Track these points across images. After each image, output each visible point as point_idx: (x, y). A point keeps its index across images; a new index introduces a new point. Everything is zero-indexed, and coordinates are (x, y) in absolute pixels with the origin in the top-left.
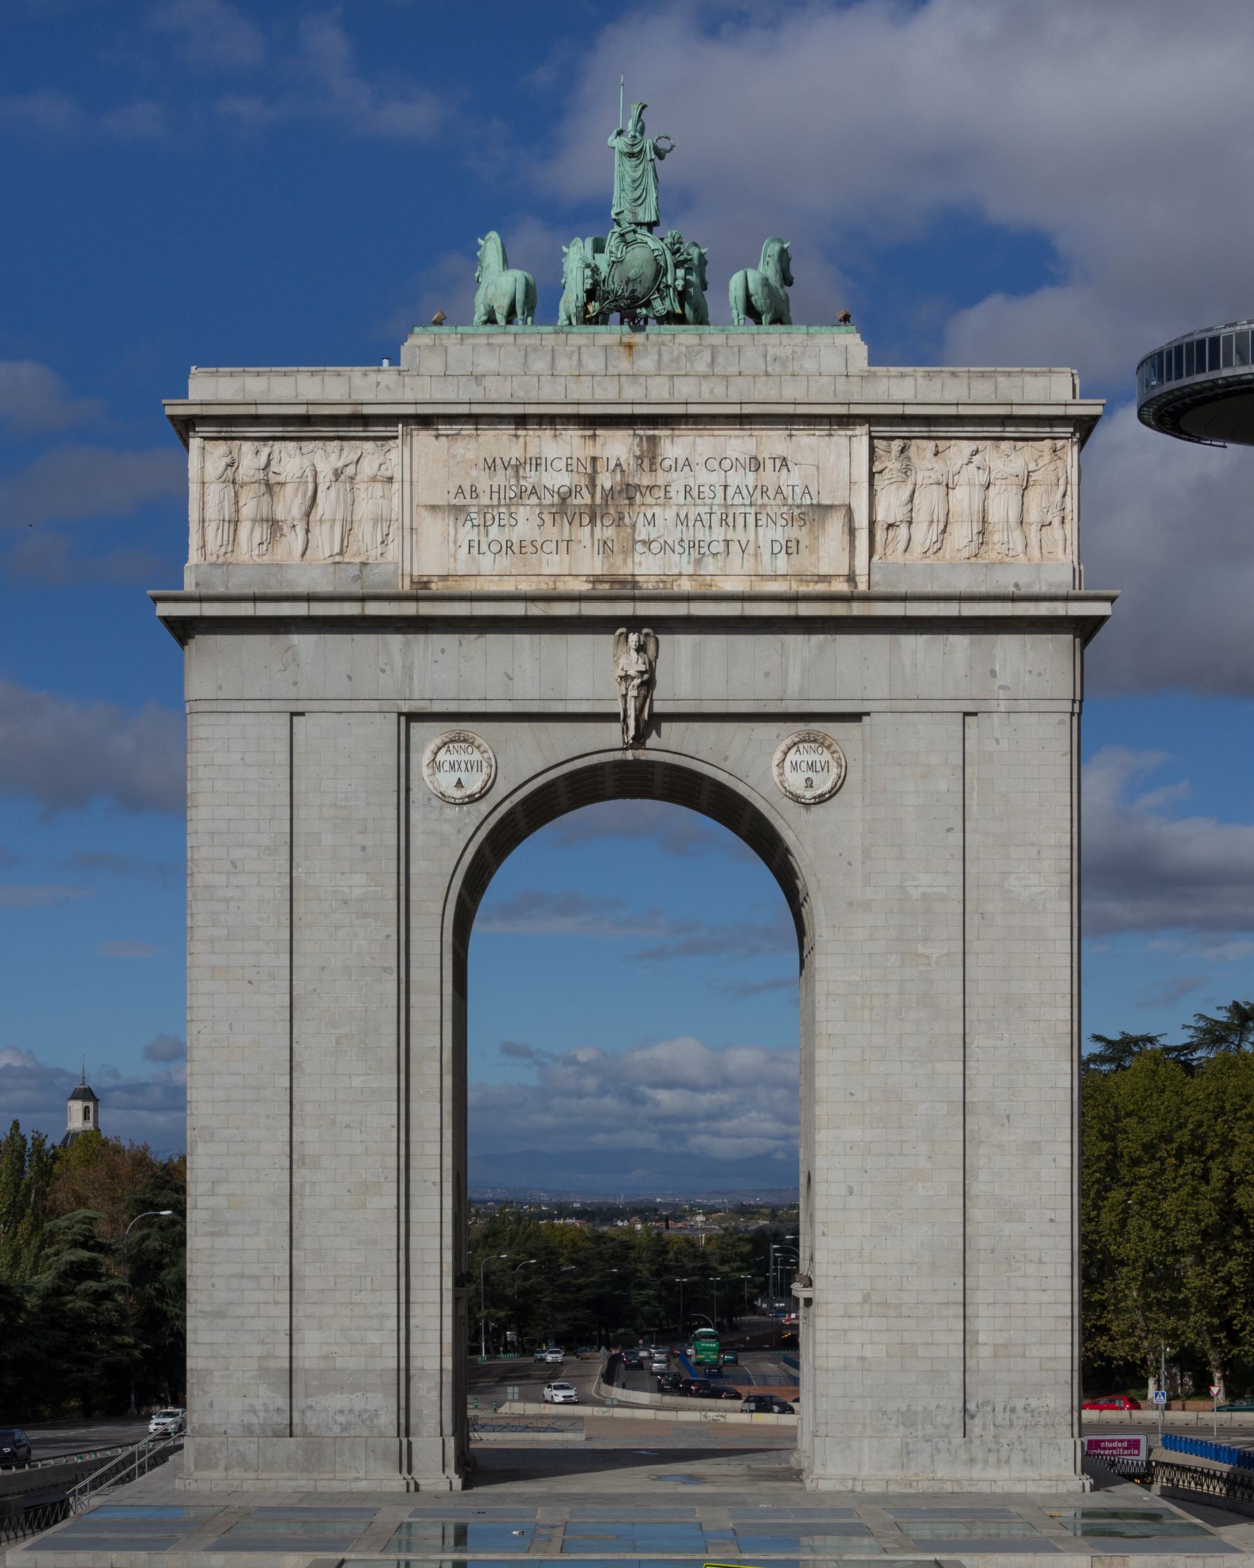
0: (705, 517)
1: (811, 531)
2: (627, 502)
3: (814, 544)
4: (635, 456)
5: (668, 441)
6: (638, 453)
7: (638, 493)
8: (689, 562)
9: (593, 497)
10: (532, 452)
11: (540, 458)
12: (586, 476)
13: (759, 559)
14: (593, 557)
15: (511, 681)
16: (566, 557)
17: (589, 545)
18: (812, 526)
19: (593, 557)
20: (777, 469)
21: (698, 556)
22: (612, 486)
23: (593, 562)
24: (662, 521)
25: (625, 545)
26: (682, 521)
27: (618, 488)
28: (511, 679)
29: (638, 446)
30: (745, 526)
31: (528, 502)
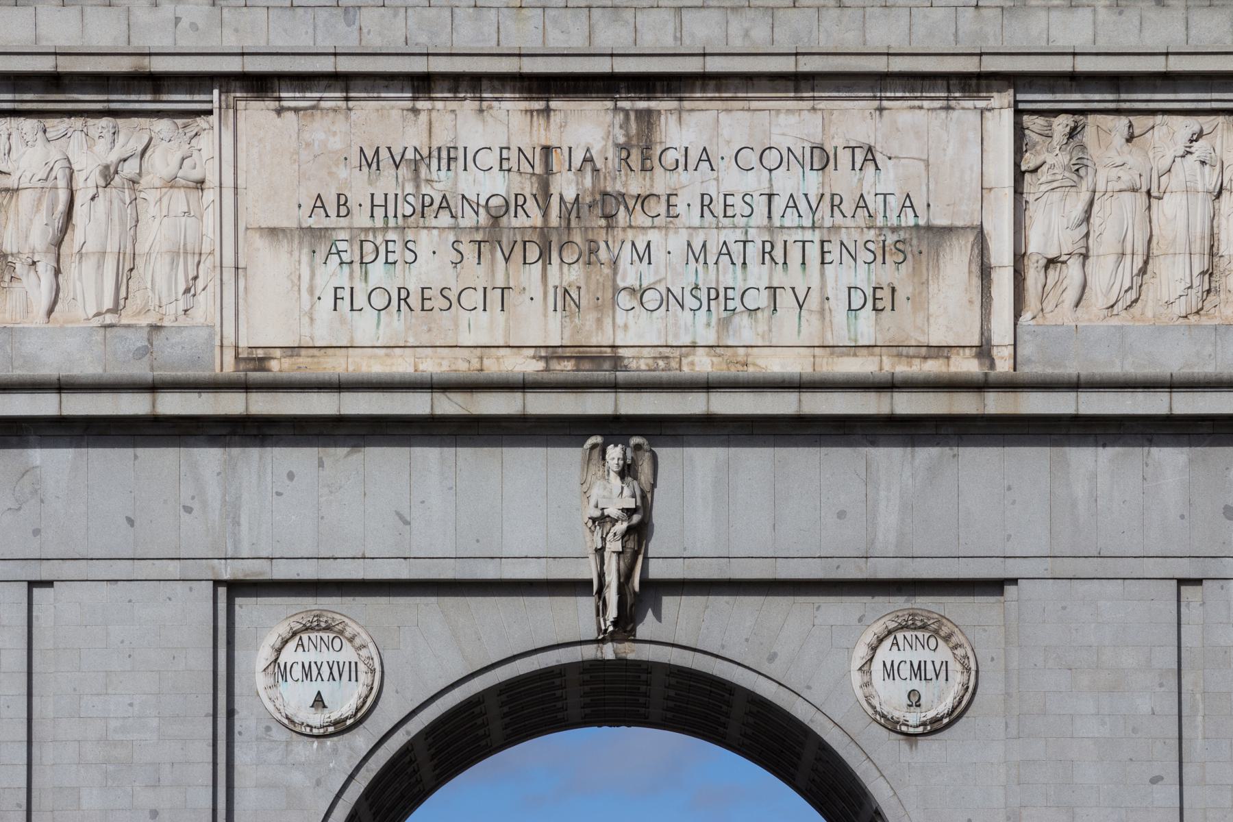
0: (736, 249)
1: (915, 271)
2: (603, 222)
3: (920, 293)
4: (617, 145)
5: (673, 119)
6: (621, 140)
7: (622, 208)
8: (708, 325)
9: (545, 215)
10: (442, 138)
11: (456, 148)
12: (534, 179)
13: (827, 319)
14: (545, 315)
15: (408, 527)
16: (501, 317)
17: (538, 296)
18: (917, 262)
19: (545, 315)
20: (858, 166)
21: (724, 315)
22: (578, 195)
23: (546, 324)
24: (663, 254)
25: (599, 295)
26: (698, 254)
27: (588, 200)
28: (407, 523)
29: (621, 127)
30: (804, 263)
31: (434, 223)
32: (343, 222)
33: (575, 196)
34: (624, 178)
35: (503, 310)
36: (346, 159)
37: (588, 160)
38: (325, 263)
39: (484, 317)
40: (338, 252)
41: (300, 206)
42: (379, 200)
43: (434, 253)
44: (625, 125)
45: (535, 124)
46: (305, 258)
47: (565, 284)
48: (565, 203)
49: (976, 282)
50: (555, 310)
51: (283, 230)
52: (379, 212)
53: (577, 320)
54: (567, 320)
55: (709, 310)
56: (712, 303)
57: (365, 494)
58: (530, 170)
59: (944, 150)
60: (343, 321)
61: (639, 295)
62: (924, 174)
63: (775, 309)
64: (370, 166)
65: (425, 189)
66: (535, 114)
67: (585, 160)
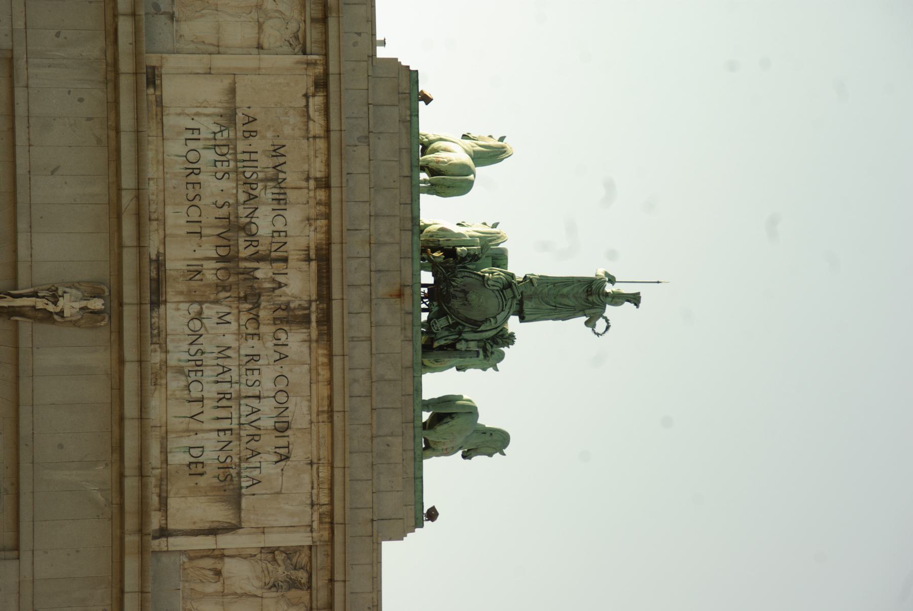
1: (213, 488)
2: (242, 294)
3: (200, 491)
4: (288, 303)
6: (292, 305)
8: (180, 361)
9: (245, 259)
11: (286, 204)
12: (268, 252)
13: (184, 434)
14: (185, 259)
15: (50, 174)
16: (183, 232)
22: (258, 279)
24: (223, 331)
27: (256, 285)
29: (300, 305)
30: (218, 419)
32: (240, 134)
35: (188, 233)
37: (280, 285)
39: (183, 221)
42: (253, 156)
43: (222, 190)
44: (301, 307)
45: (301, 253)
48: (253, 271)
49: (207, 526)
50: (188, 265)
52: (246, 157)
53: (182, 279)
54: (182, 273)
56: (193, 363)
57: (70, 147)
58: (273, 250)
61: (197, 317)
63: (190, 402)
64: (274, 151)
65: (260, 185)
66: (307, 252)
67: (280, 283)
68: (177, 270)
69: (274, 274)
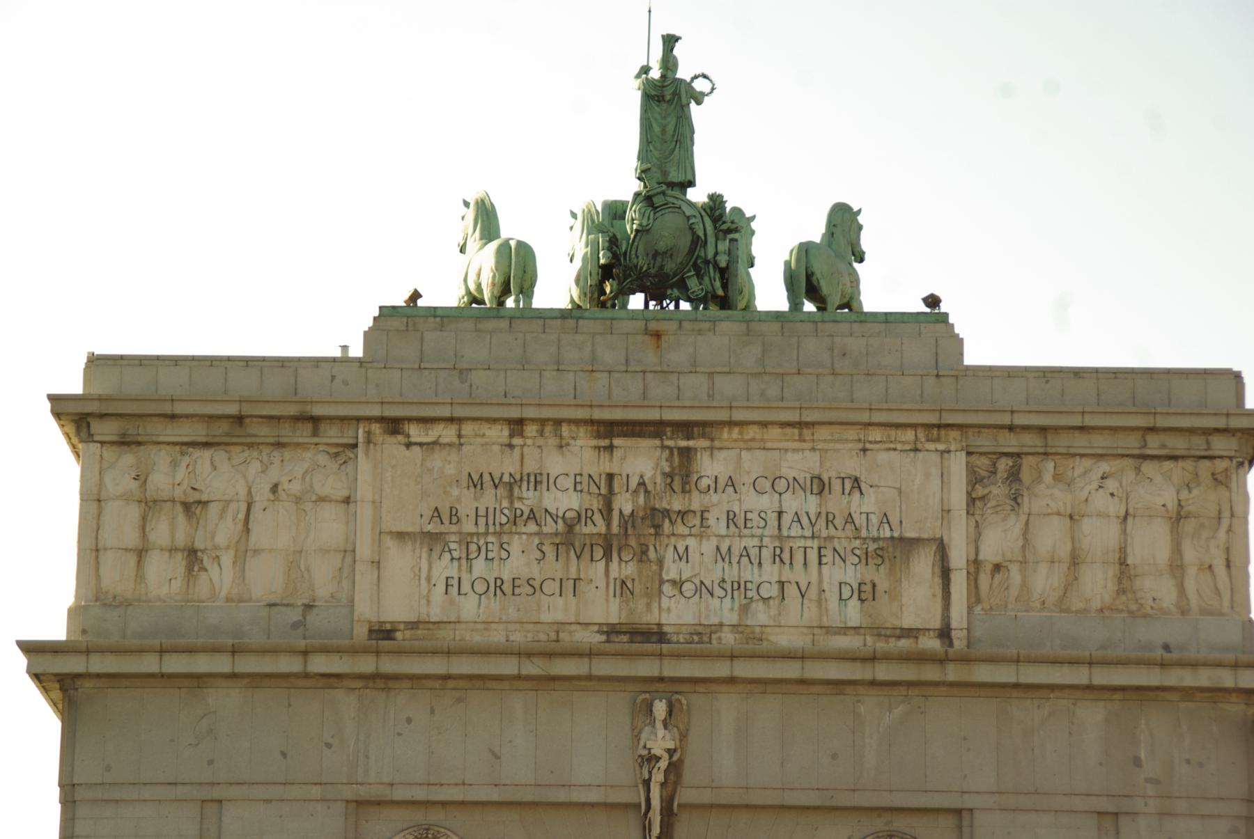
2: (652, 531)
5: (706, 455)
6: (667, 470)
8: (732, 609)
9: (609, 526)
11: (541, 474)
12: (600, 498)
13: (824, 606)
14: (607, 600)
15: (498, 761)
20: (847, 491)
22: (633, 510)
24: (697, 555)
25: (649, 585)
27: (641, 514)
30: (805, 564)
33: (630, 511)
34: (668, 498)
35: (574, 595)
36: (457, 481)
38: (440, 558)
39: (560, 601)
40: (450, 551)
41: (421, 516)
43: (523, 552)
46: (424, 555)
47: (622, 577)
51: (408, 534)
52: (482, 521)
55: (733, 598)
58: (597, 491)
59: (913, 481)
60: (452, 602)
61: (679, 586)
62: (898, 498)
63: (783, 598)
67: (639, 484)
68: (620, 609)
69: (627, 491)
